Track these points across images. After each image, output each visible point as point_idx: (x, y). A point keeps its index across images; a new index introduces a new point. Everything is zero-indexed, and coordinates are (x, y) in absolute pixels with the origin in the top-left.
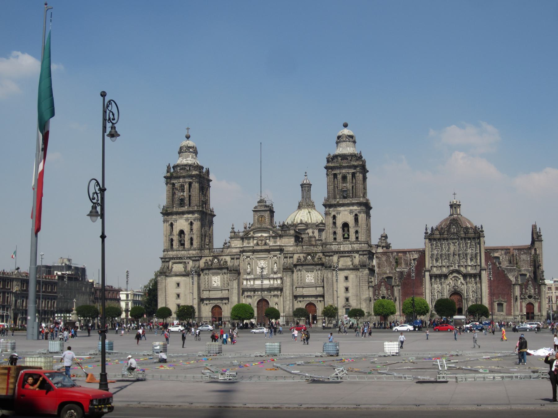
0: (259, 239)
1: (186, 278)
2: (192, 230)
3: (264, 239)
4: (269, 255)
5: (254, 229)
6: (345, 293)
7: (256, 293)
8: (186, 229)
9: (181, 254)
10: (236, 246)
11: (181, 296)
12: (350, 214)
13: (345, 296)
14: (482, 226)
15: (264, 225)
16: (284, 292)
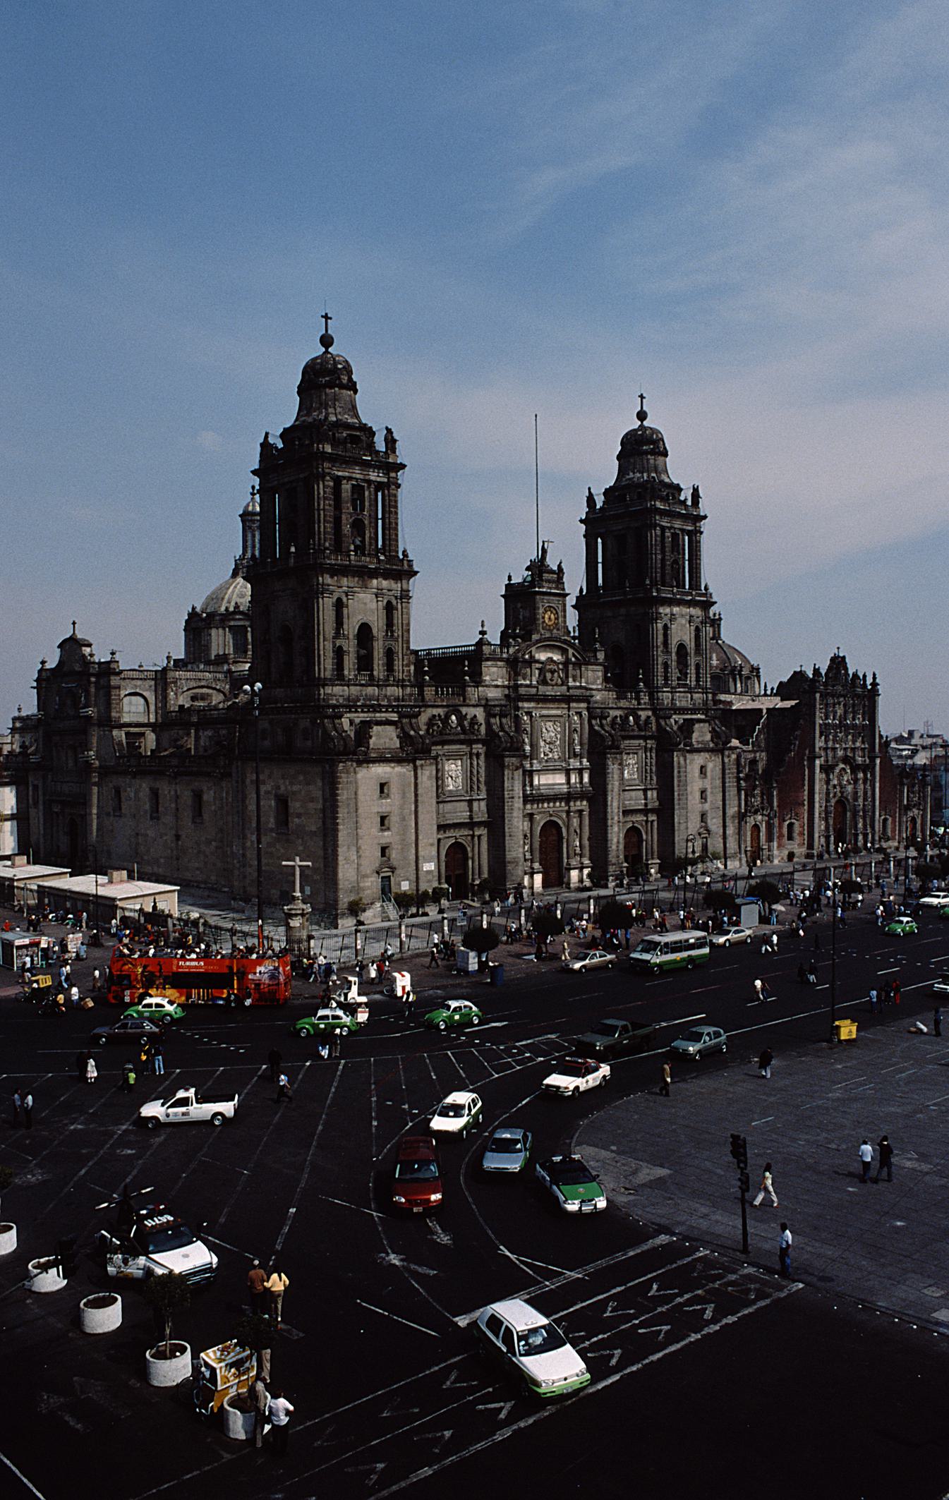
0: (548, 667)
1: (405, 770)
2: (390, 624)
3: (556, 667)
4: (565, 711)
5: (538, 641)
6: (702, 803)
7: (540, 805)
8: (378, 625)
9: (366, 695)
10: (495, 683)
11: (394, 820)
12: (688, 625)
13: (700, 810)
14: (874, 675)
15: (555, 631)
16: (609, 803)
